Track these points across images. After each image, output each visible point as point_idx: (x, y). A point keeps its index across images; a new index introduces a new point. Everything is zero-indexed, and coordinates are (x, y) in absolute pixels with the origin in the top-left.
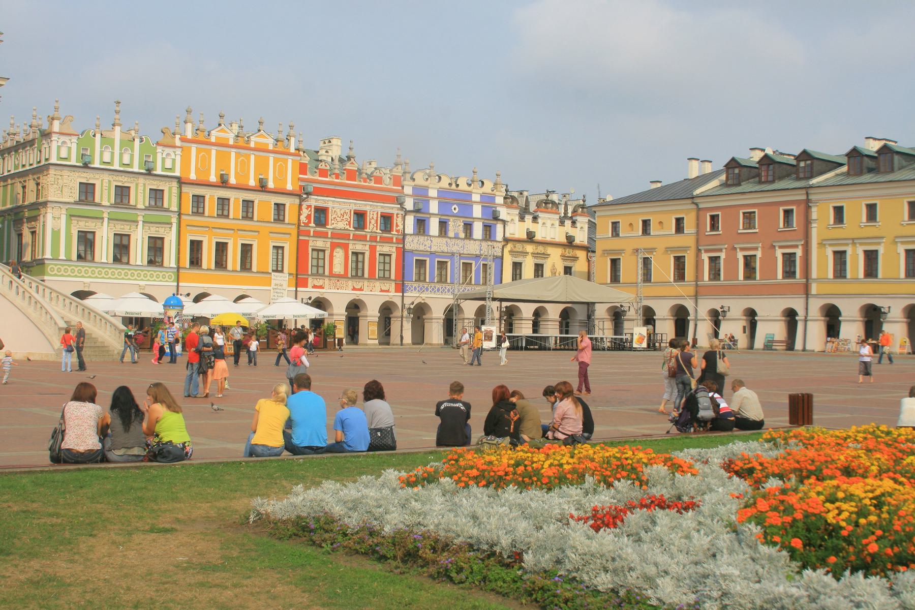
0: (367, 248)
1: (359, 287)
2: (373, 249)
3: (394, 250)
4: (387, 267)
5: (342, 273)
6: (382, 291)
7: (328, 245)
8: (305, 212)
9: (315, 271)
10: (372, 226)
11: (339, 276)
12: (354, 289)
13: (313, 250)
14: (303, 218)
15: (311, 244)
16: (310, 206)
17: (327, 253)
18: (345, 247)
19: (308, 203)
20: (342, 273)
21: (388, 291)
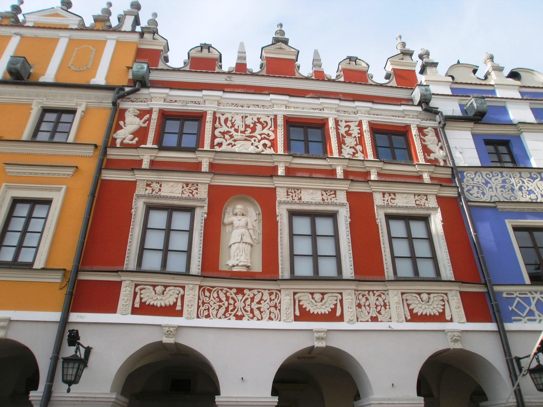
0: (342, 198)
1: (325, 310)
2: (361, 205)
3: (433, 202)
4: (422, 249)
5: (258, 267)
6: (415, 317)
7: (203, 193)
8: (132, 123)
9: (152, 261)
10: (347, 152)
11: (248, 276)
12: (304, 315)
13: (150, 208)
14: (124, 134)
15: (140, 190)
16: (150, 112)
17: (200, 215)
18: (266, 200)
19: (144, 106)
20: (258, 267)
21: (441, 317)
